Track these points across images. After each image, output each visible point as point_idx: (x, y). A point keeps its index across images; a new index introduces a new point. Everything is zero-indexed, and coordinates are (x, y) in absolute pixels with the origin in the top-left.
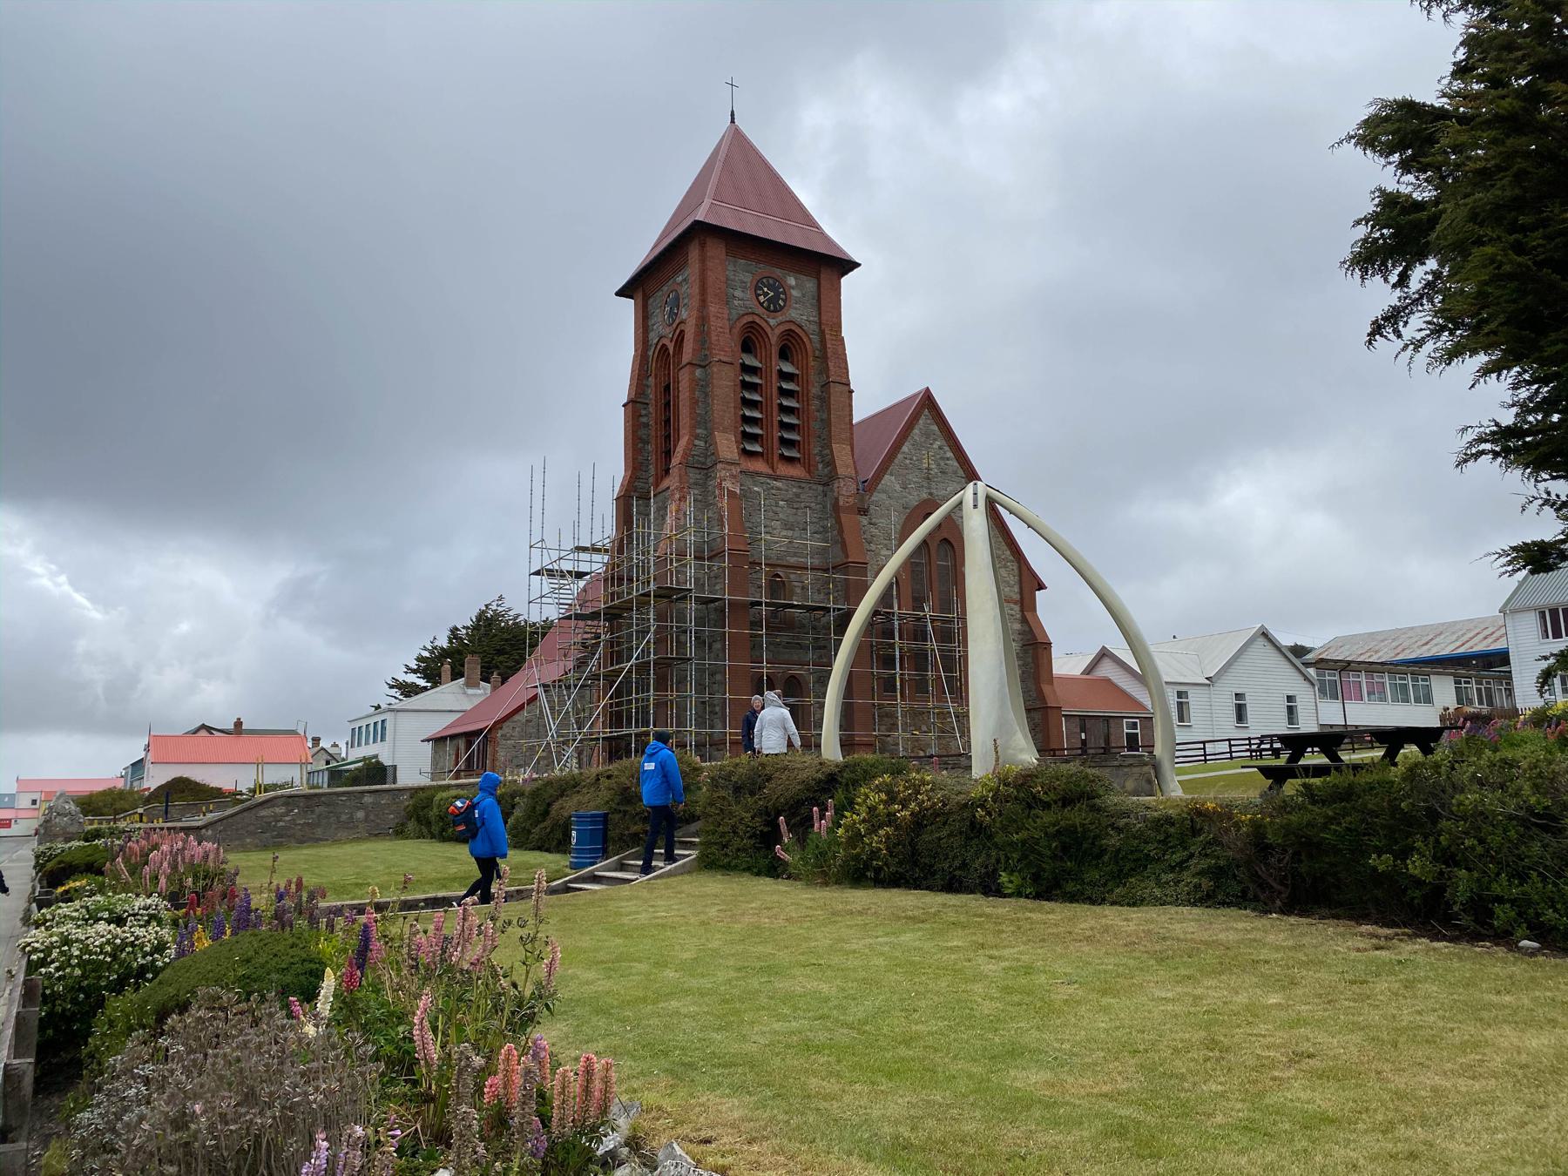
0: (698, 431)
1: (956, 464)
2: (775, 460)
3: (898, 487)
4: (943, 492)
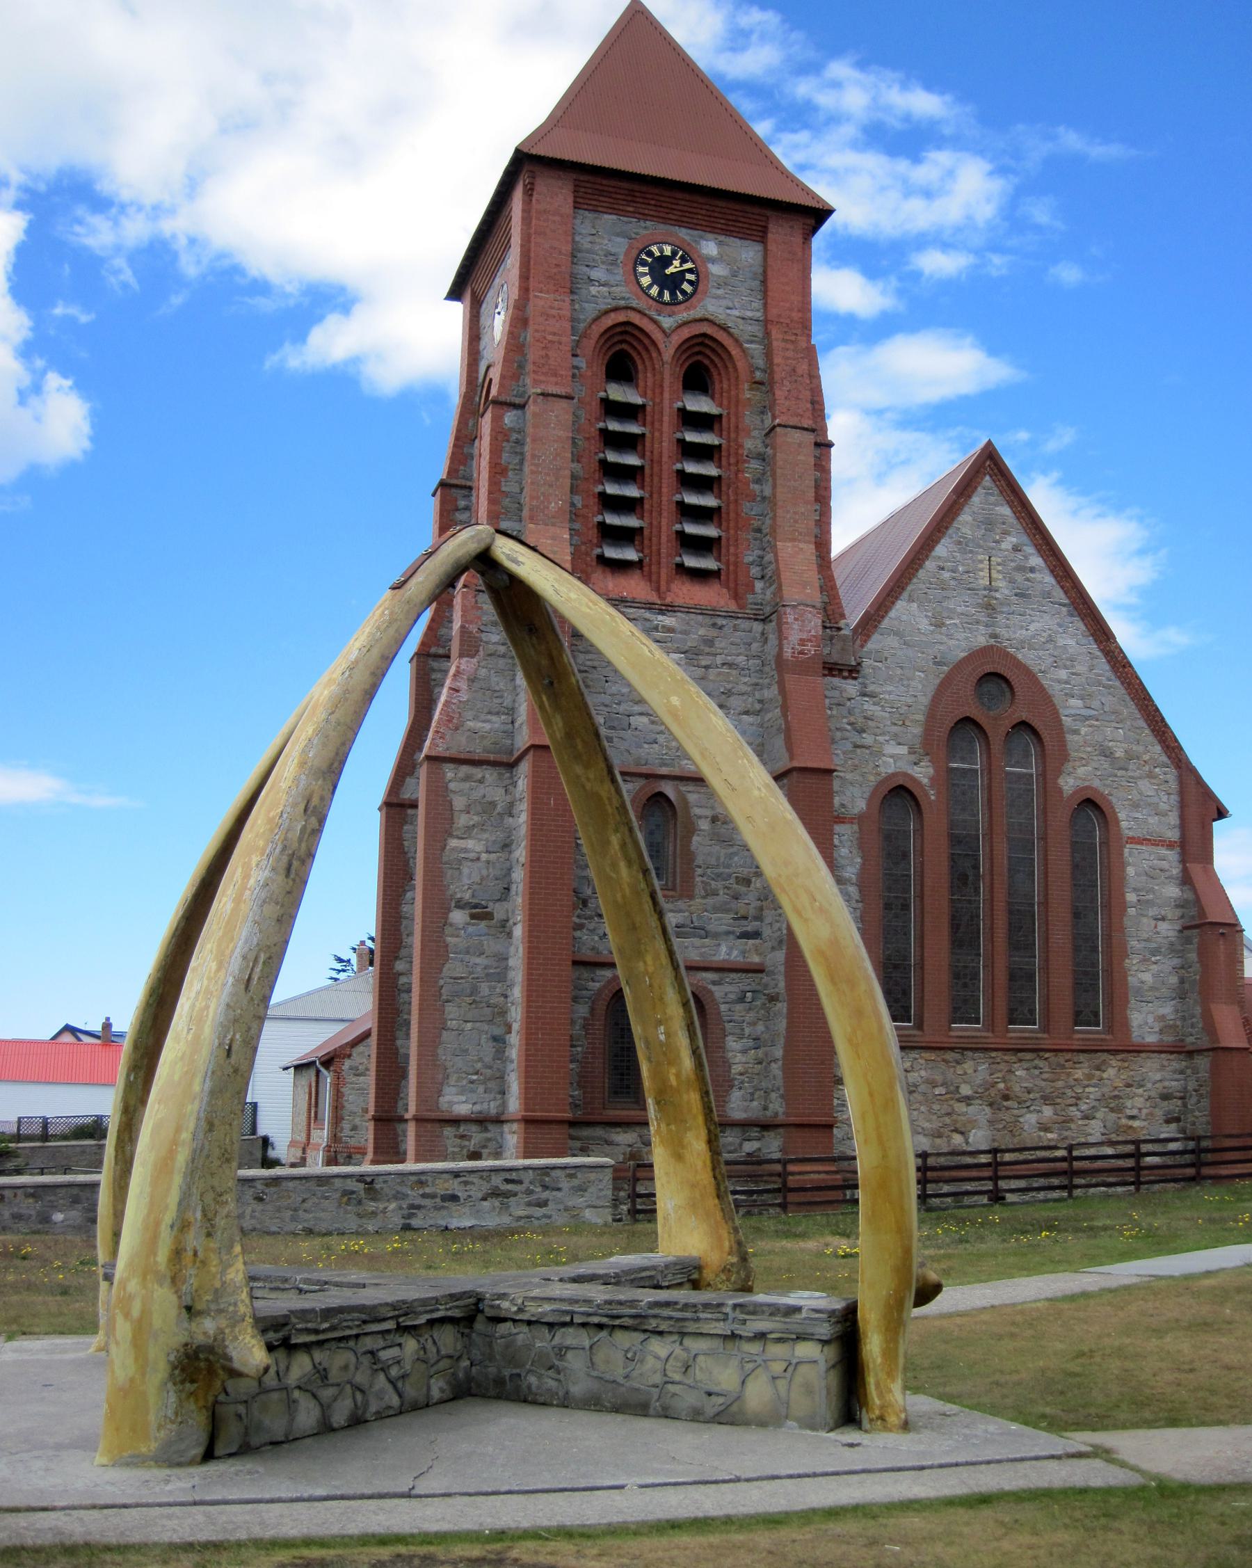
1: (1049, 579)
2: (664, 572)
3: (924, 625)
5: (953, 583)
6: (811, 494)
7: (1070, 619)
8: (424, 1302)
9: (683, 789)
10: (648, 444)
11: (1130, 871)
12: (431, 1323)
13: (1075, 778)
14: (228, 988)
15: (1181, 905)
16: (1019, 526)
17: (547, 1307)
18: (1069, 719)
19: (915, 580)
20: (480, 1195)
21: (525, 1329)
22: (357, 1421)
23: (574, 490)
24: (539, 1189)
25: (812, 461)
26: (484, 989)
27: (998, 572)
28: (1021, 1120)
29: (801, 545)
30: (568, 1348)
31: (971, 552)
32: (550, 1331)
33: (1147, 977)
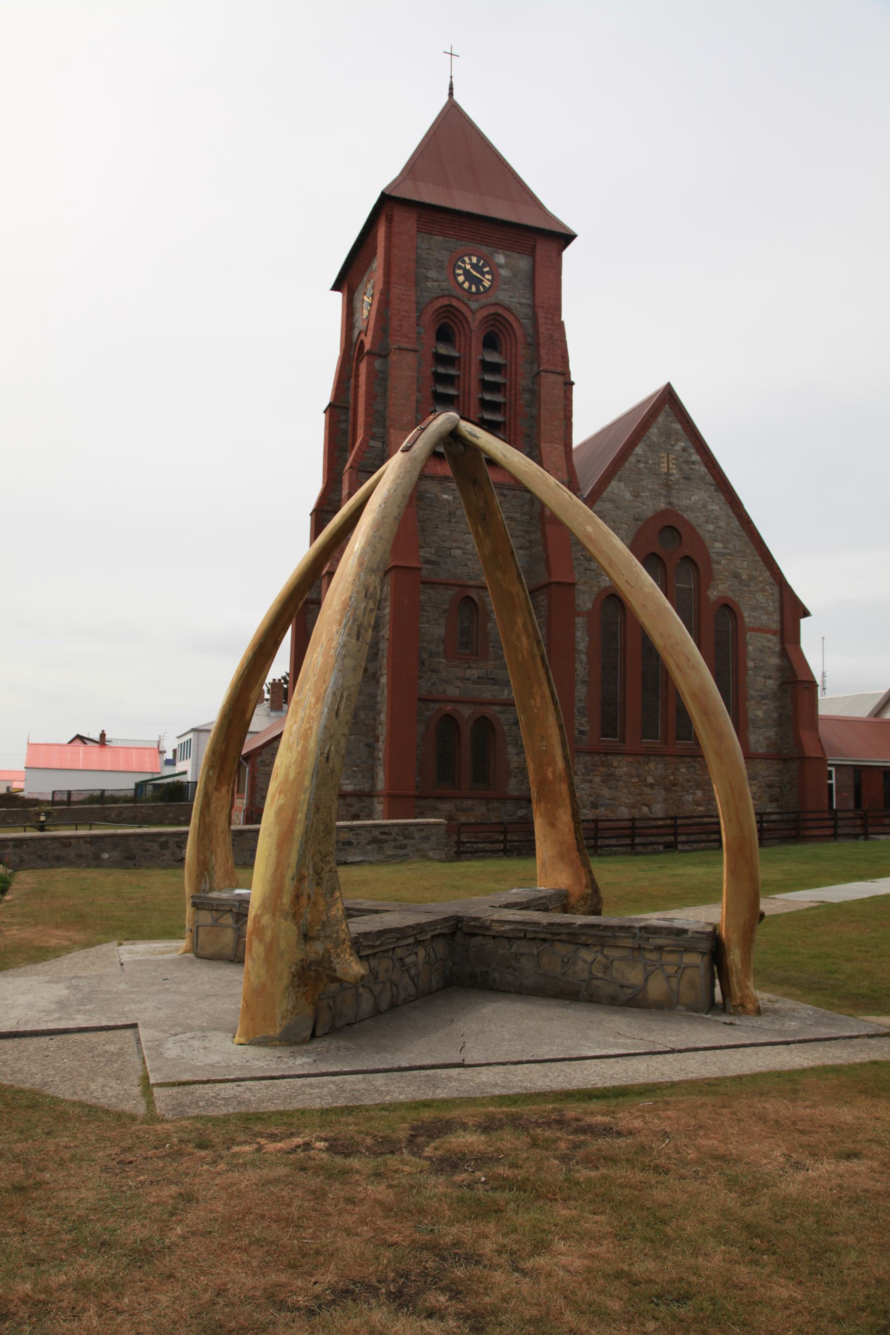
0: (375, 430)
1: (703, 469)
3: (628, 496)
4: (686, 502)
5: (645, 470)
6: (561, 414)
7: (716, 494)
8: (430, 924)
9: (482, 594)
10: (462, 382)
11: (750, 648)
12: (433, 937)
13: (718, 591)
14: (324, 716)
15: (781, 669)
16: (686, 436)
17: (508, 927)
18: (714, 555)
19: (623, 468)
20: (365, 842)
21: (492, 941)
22: (393, 1006)
23: (417, 410)
24: (401, 838)
25: (562, 393)
26: (362, 715)
27: (673, 464)
28: (683, 798)
29: (556, 446)
30: (522, 954)
31: (657, 451)
32: (509, 944)
33: (760, 713)
